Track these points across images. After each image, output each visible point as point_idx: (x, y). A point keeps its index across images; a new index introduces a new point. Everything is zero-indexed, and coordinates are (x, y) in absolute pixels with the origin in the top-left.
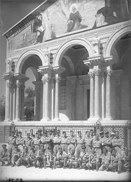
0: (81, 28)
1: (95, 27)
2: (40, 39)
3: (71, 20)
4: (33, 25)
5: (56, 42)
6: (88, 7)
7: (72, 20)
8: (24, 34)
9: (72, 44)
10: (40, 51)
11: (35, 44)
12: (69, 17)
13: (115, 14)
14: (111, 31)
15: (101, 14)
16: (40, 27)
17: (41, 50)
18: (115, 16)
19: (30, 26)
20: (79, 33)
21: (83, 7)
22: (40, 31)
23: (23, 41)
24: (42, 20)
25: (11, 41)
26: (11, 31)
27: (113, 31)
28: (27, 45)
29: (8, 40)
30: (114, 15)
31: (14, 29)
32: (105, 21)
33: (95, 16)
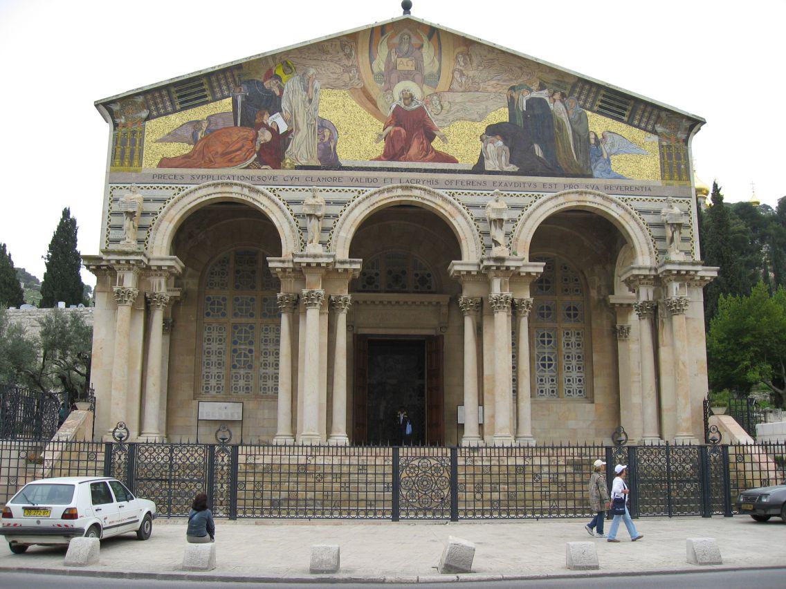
0: (434, 160)
1: (479, 169)
2: (274, 153)
3: (396, 125)
4: (239, 100)
5: (339, 179)
6: (457, 107)
7: (401, 126)
8: (198, 122)
9: (401, 201)
10: (271, 194)
11: (248, 167)
12: (390, 113)
13: (538, 151)
14: (530, 194)
15: (498, 137)
16: (271, 114)
17: (277, 192)
18: (540, 156)
19: (229, 100)
20: (426, 171)
21: (440, 102)
22: (271, 130)
23: (190, 144)
24: (280, 97)
25: (134, 133)
26: (140, 99)
27: (536, 194)
28: (210, 164)
29: (116, 125)
30: (536, 153)
31: (157, 94)
32: (511, 162)
33: (481, 137)
